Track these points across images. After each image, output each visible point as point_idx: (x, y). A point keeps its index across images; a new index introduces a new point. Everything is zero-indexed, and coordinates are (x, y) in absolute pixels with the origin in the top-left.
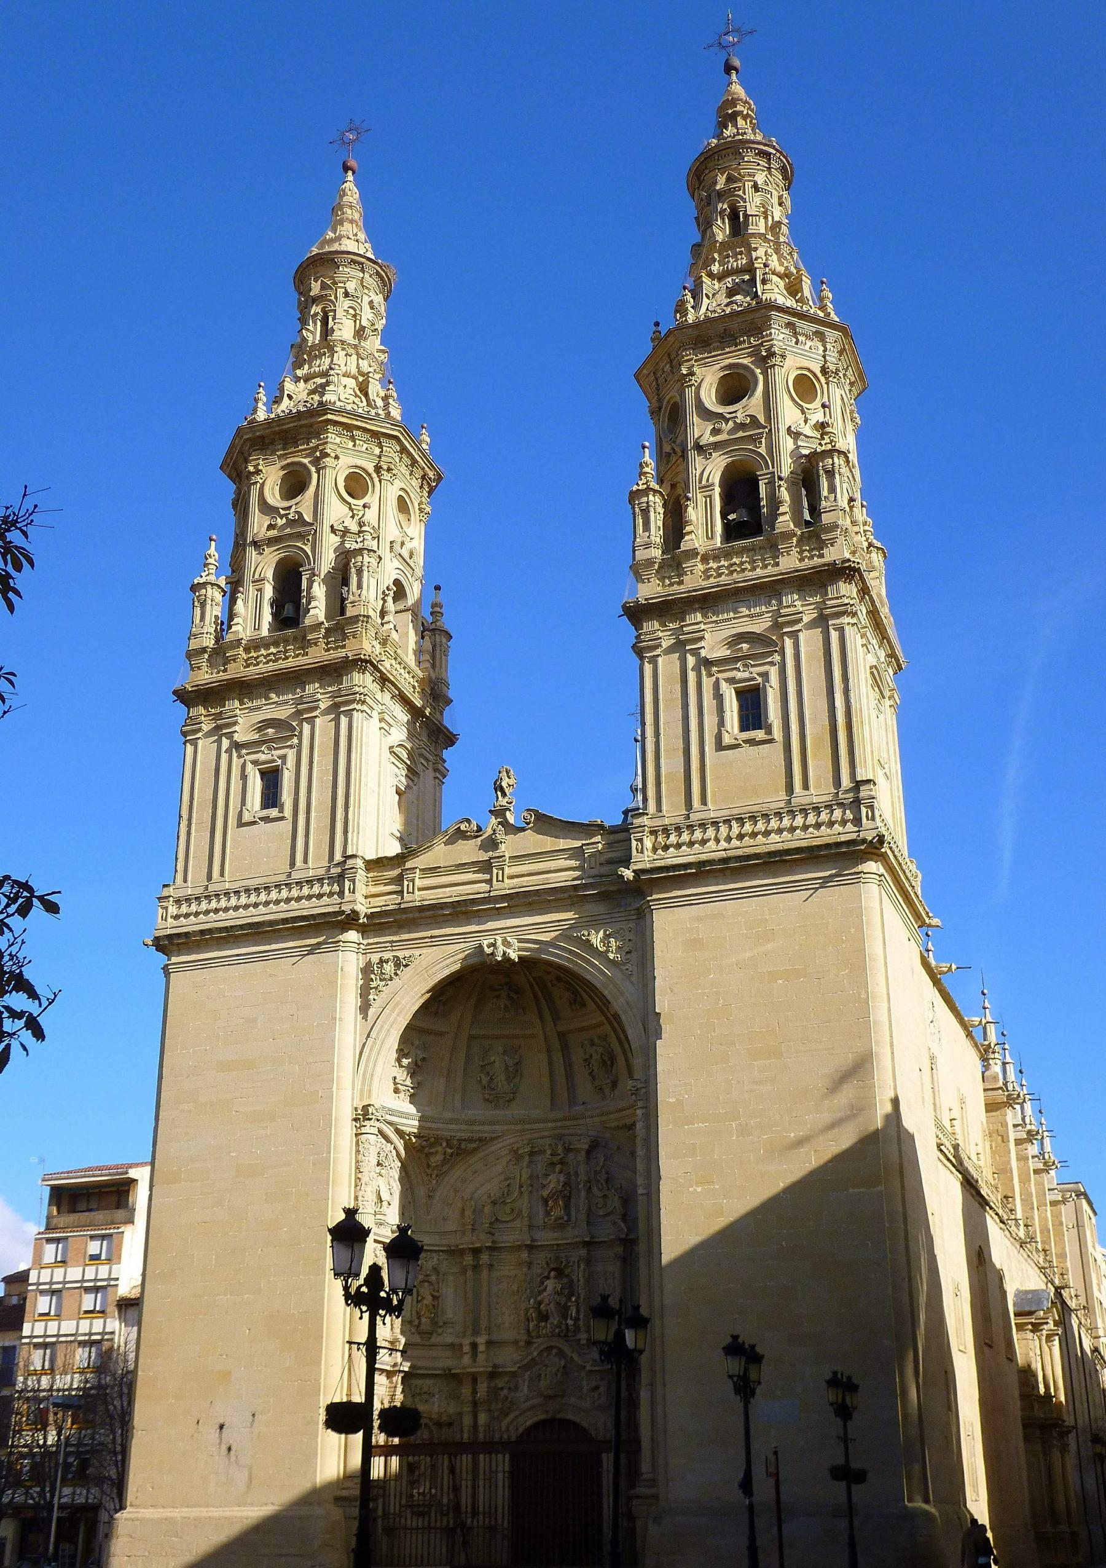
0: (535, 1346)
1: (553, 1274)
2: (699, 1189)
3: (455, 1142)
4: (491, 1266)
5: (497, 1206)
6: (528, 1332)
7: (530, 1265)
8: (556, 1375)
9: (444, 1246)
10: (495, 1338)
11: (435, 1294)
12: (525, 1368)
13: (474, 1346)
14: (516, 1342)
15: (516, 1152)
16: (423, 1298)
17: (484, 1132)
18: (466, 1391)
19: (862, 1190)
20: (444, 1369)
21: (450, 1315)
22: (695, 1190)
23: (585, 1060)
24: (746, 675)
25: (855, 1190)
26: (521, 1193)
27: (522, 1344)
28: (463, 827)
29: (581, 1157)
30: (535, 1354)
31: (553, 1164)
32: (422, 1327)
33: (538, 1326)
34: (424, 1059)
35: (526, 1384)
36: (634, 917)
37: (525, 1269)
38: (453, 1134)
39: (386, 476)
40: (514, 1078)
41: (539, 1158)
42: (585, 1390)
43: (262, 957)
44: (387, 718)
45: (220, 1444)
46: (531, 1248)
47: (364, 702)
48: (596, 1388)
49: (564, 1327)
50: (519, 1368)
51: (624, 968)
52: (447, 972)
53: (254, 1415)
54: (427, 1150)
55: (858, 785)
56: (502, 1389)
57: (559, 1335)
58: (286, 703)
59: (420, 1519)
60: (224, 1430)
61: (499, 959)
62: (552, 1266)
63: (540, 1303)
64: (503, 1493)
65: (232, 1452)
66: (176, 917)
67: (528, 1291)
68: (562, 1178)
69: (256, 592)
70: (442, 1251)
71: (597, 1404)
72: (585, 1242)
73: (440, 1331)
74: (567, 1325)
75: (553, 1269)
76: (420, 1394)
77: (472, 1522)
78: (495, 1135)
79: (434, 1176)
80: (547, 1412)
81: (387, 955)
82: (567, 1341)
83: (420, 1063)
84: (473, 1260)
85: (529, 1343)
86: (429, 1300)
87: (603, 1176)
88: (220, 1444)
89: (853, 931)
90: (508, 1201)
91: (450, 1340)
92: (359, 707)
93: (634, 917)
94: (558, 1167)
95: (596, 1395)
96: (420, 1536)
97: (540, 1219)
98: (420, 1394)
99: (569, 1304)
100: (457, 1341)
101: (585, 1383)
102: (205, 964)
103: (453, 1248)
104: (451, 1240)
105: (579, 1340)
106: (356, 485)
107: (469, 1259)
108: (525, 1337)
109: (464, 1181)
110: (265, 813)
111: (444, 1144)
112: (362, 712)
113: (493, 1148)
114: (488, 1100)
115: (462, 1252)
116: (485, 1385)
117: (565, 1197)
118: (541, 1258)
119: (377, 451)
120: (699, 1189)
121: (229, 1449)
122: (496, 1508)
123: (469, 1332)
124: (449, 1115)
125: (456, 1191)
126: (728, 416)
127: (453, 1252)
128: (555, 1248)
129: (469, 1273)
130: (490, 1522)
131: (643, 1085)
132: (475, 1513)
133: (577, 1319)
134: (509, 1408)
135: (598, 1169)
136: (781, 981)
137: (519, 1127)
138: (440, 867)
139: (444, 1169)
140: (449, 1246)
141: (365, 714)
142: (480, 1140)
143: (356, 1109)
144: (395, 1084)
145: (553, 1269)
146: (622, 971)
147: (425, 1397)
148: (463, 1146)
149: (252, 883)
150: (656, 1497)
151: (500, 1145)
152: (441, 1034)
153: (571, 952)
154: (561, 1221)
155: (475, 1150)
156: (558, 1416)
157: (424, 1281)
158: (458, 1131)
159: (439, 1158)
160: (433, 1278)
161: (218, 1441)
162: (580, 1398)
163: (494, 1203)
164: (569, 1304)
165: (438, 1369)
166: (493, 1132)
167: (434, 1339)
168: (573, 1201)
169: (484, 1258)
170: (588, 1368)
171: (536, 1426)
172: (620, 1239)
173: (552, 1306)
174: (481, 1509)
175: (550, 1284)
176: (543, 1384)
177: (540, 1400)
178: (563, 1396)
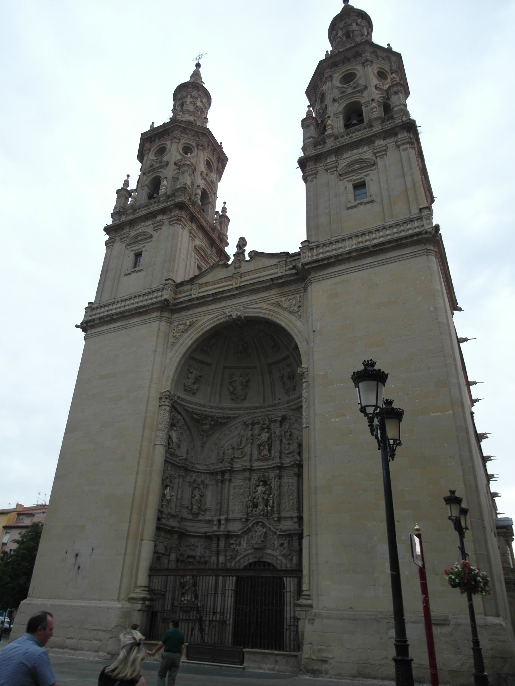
0: (250, 521)
1: (261, 483)
2: (337, 420)
3: (215, 418)
4: (230, 481)
5: (235, 451)
6: (247, 514)
7: (250, 479)
8: (261, 536)
9: (208, 470)
10: (231, 516)
11: (202, 494)
12: (246, 532)
13: (219, 521)
14: (241, 519)
15: (245, 423)
16: (195, 496)
17: (230, 414)
18: (214, 545)
19: (439, 414)
20: (203, 533)
21: (208, 506)
23: (280, 377)
24: (359, 177)
25: (435, 414)
26: (247, 444)
27: (243, 520)
29: (278, 424)
30: (250, 525)
31: (264, 429)
32: (194, 511)
33: (252, 511)
34: (200, 376)
35: (245, 542)
36: (303, 291)
37: (247, 481)
38: (214, 414)
39: (200, 148)
40: (246, 388)
41: (256, 426)
42: (276, 546)
43: (124, 328)
44: (193, 232)
45: (75, 564)
46: (251, 470)
47: (180, 220)
48: (282, 545)
49: (265, 511)
50: (241, 533)
51: (296, 315)
52: (209, 327)
53: (93, 549)
54: (201, 422)
56: (232, 544)
57: (263, 515)
58: (149, 225)
59: (184, 614)
60: (78, 557)
61: (234, 317)
62: (261, 479)
63: (254, 498)
64: (230, 601)
65: (80, 569)
66: (91, 316)
67: (248, 492)
68: (267, 435)
70: (207, 473)
71: (282, 553)
72: (278, 466)
73: (203, 513)
74: (267, 509)
75: (261, 481)
76: (190, 546)
77: (213, 617)
78: (235, 416)
79: (205, 436)
80: (256, 557)
81: (181, 323)
82: (268, 519)
83: (198, 378)
84: (222, 477)
85: (247, 520)
86: (198, 497)
87: (289, 433)
88: (75, 564)
90: (240, 448)
91: (207, 518)
92: (179, 222)
93: (303, 291)
94: (266, 430)
95: (282, 548)
96: (187, 625)
97: (255, 456)
98: (190, 546)
99: (269, 498)
100: (210, 518)
101: (276, 542)
102: (101, 333)
103: (212, 471)
104: (212, 468)
105: (273, 518)
106: (187, 150)
107: (219, 477)
108: (245, 516)
109: (220, 439)
110: (134, 270)
111: (210, 419)
112: (180, 224)
113: (235, 423)
114: (232, 399)
115: (217, 473)
116: (223, 542)
117: (268, 445)
118: (255, 476)
119: (197, 139)
121: (79, 568)
122: (227, 609)
123: (218, 514)
124: (212, 404)
125: (216, 444)
126: (347, 87)
127: (212, 474)
128: (263, 470)
129: (220, 484)
130: (179, 616)
131: (306, 370)
132: (214, 613)
133: (273, 507)
134: (236, 555)
135: (286, 430)
137: (247, 411)
138: (209, 282)
139: (210, 433)
140: (210, 470)
141: (181, 226)
142: (228, 418)
144: (185, 386)
145: (261, 481)
146: (296, 316)
147: (192, 547)
148: (219, 421)
150: (311, 606)
151: (238, 421)
152: (209, 364)
153: (270, 310)
154: (266, 457)
155: (225, 424)
156: (261, 560)
157: (196, 488)
158: (217, 413)
159: (208, 426)
160: (201, 486)
162: (273, 550)
163: (233, 448)
164: (269, 498)
165: (200, 533)
166: (234, 414)
167: (201, 517)
168: (273, 447)
169: (227, 476)
170: (278, 533)
171: (250, 564)
172: (296, 464)
173: (260, 500)
174: (219, 610)
175: (260, 489)
176: (253, 542)
177: (252, 551)
178: (264, 549)
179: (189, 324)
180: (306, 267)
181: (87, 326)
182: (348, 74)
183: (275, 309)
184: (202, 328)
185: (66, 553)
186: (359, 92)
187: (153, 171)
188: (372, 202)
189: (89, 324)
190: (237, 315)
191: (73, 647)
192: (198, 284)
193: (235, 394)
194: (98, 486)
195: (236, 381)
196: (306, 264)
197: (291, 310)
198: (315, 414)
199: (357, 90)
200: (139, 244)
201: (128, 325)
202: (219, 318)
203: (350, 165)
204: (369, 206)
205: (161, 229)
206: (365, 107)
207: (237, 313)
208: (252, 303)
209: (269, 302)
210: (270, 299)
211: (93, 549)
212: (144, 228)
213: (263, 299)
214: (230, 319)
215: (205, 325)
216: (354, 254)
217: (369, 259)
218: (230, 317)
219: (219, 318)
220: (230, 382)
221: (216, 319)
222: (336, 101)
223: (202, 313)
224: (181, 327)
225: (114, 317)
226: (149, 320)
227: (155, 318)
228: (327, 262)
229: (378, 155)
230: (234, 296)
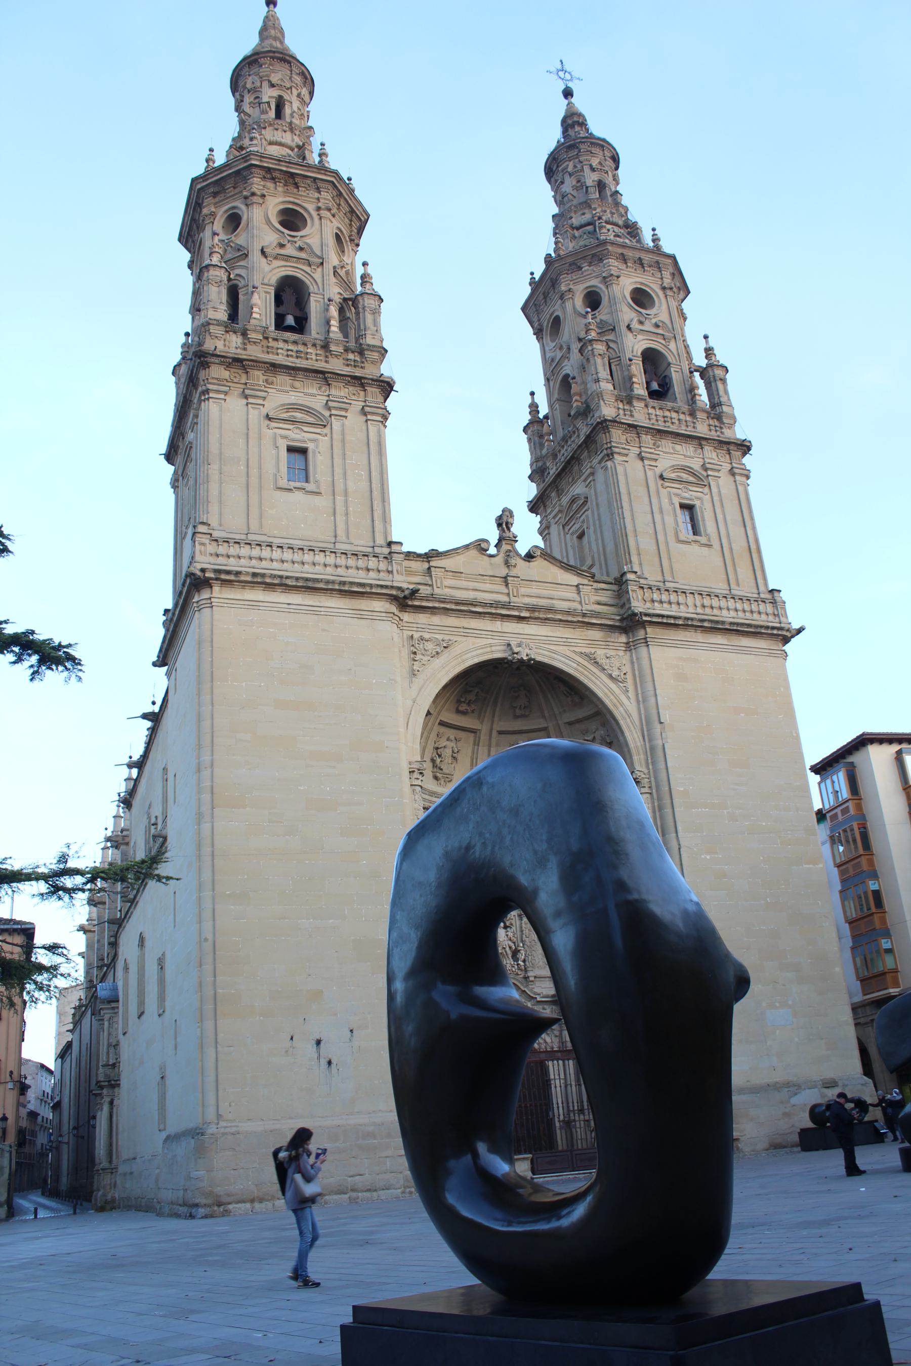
2: (708, 857)
19: (811, 866)
22: (705, 857)
25: (807, 866)
28: (483, 546)
43: (313, 611)
51: (621, 685)
52: (477, 660)
53: (351, 1031)
55: (772, 591)
60: (322, 1044)
65: (333, 1066)
69: (264, 294)
74: (518, 965)
81: (427, 636)
88: (319, 1058)
89: (782, 689)
93: (624, 649)
102: (254, 605)
114: (436, 778)
120: (708, 857)
121: (330, 1063)
131: (644, 776)
136: (743, 715)
138: (461, 573)
143: (410, 763)
146: (619, 687)
149: (297, 543)
153: (579, 664)
161: (316, 1056)
173: (508, 949)
179: (445, 645)
180: (645, 618)
181: (217, 579)
182: (640, 288)
183: (586, 663)
184: (464, 657)
185: (292, 1038)
186: (664, 339)
187: (286, 261)
188: (709, 546)
189: (223, 577)
190: (527, 655)
191: (369, 1187)
192: (443, 570)
193: (442, 769)
194: (331, 921)
195: (445, 747)
196: (646, 615)
197: (614, 674)
198: (679, 845)
199: (663, 335)
200: (297, 428)
201: (322, 609)
202: (494, 648)
203: (675, 468)
204: (705, 550)
205: (346, 417)
206: (675, 371)
207: (529, 652)
208: (548, 642)
209: (577, 649)
210: (575, 644)
211: (351, 1031)
212: (302, 395)
213: (565, 640)
214: (514, 658)
215: (470, 655)
216: (706, 624)
217: (720, 637)
218: (515, 655)
219: (494, 648)
220: (437, 748)
221: (489, 649)
222: (632, 332)
223: (462, 630)
224: (430, 646)
225: (289, 582)
226: (370, 613)
227: (384, 614)
228: (672, 622)
229: (710, 473)
230: (520, 619)
